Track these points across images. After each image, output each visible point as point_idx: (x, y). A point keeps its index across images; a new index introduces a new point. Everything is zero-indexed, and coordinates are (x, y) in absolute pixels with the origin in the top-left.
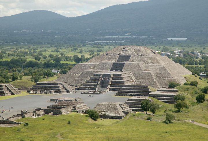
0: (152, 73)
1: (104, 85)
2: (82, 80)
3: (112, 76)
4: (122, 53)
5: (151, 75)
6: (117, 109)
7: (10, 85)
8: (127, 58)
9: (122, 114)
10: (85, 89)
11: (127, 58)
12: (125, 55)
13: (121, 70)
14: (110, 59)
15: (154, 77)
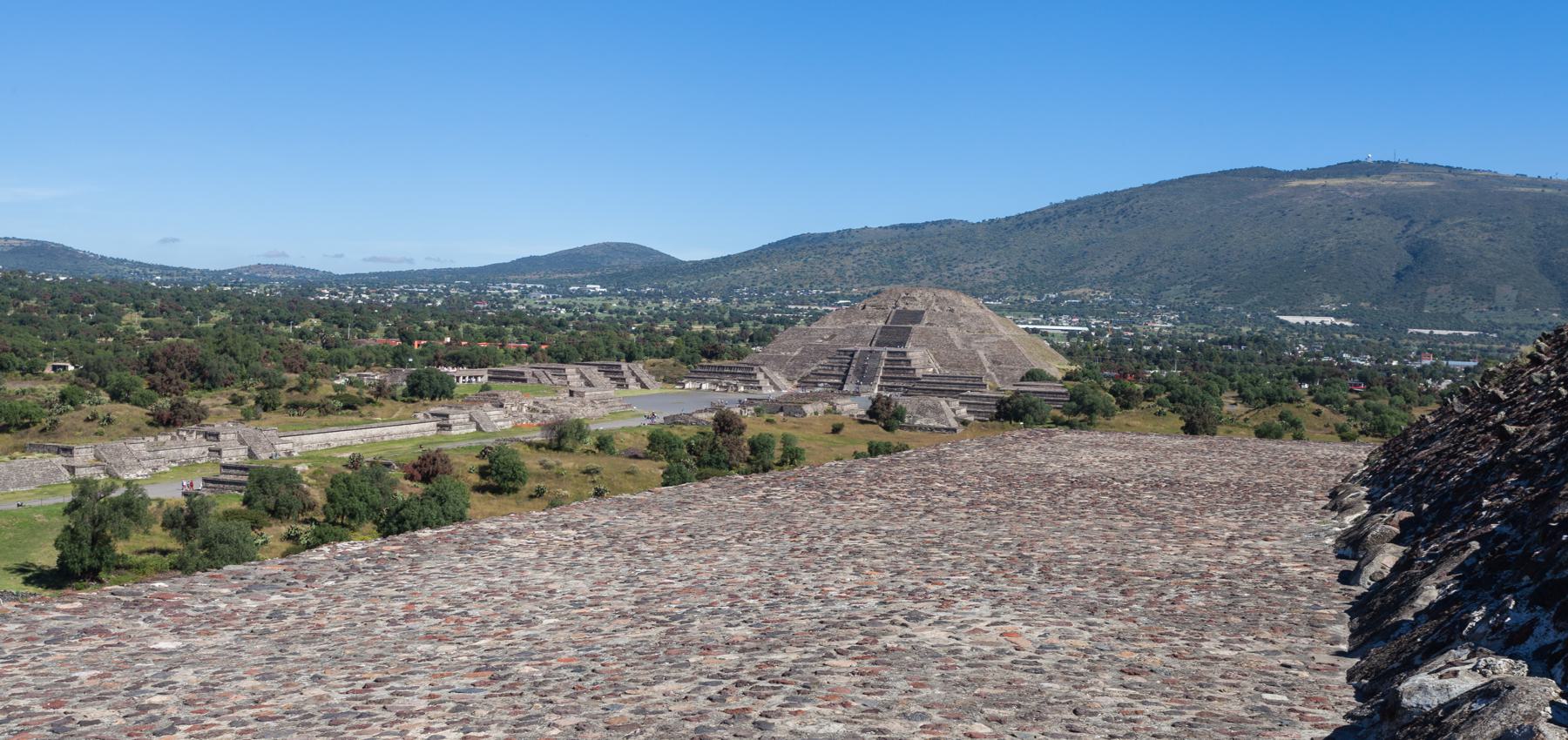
0: (981, 353)
1: (865, 376)
2: (803, 366)
3: (885, 355)
4: (902, 305)
5: (977, 358)
6: (942, 411)
7: (638, 367)
8: (917, 317)
9: (954, 424)
10: (816, 384)
11: (917, 317)
12: (910, 308)
13: (903, 344)
14: (873, 318)
15: (987, 364)
